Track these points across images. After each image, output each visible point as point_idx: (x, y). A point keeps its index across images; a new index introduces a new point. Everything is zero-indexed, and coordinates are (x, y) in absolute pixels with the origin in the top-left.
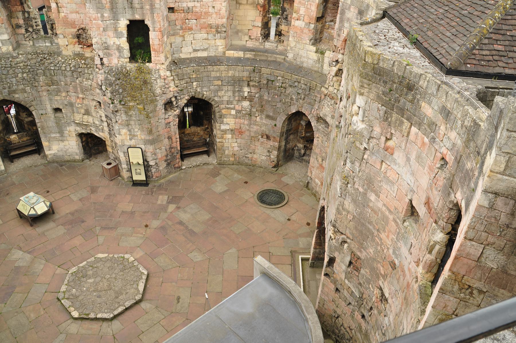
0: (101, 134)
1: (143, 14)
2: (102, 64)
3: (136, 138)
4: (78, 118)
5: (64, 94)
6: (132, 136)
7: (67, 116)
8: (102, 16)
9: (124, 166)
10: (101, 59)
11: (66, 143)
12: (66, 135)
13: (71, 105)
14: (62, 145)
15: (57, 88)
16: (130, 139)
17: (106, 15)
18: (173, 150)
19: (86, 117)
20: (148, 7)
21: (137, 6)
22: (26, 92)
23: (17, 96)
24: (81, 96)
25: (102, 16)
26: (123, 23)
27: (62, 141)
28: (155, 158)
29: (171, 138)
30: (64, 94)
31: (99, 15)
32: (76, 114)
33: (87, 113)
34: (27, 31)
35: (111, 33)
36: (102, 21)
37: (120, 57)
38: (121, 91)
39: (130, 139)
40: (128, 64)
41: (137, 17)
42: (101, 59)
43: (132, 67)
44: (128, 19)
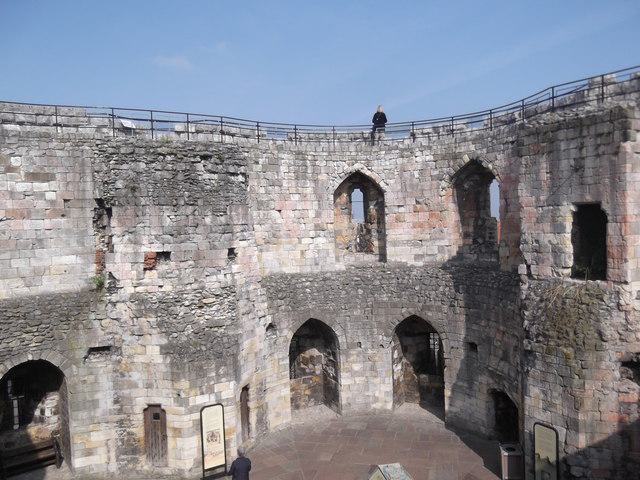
0: (515, 394)
1: (599, 193)
2: (529, 275)
3: (552, 409)
4: (493, 363)
5: (483, 323)
6: (548, 406)
7: (481, 358)
8: (538, 200)
9: (528, 459)
10: (529, 267)
11: (474, 401)
12: (475, 388)
13: (489, 340)
14: (468, 401)
15: (478, 313)
16: (545, 410)
17: (542, 198)
18: (629, 465)
19: (502, 363)
20: (607, 181)
21: (589, 180)
22: (441, 311)
23: (430, 314)
24: (501, 328)
25: (538, 200)
26: (567, 213)
27: (470, 396)
28: (584, 463)
29: (629, 437)
30: (483, 323)
31: (534, 199)
32: (492, 357)
33: (505, 358)
34: (475, 241)
35: (547, 227)
36: (537, 207)
37: (557, 264)
38: (543, 318)
39: (545, 410)
40: (570, 280)
41: (589, 198)
42: (529, 267)
43: (571, 285)
44: (573, 204)
